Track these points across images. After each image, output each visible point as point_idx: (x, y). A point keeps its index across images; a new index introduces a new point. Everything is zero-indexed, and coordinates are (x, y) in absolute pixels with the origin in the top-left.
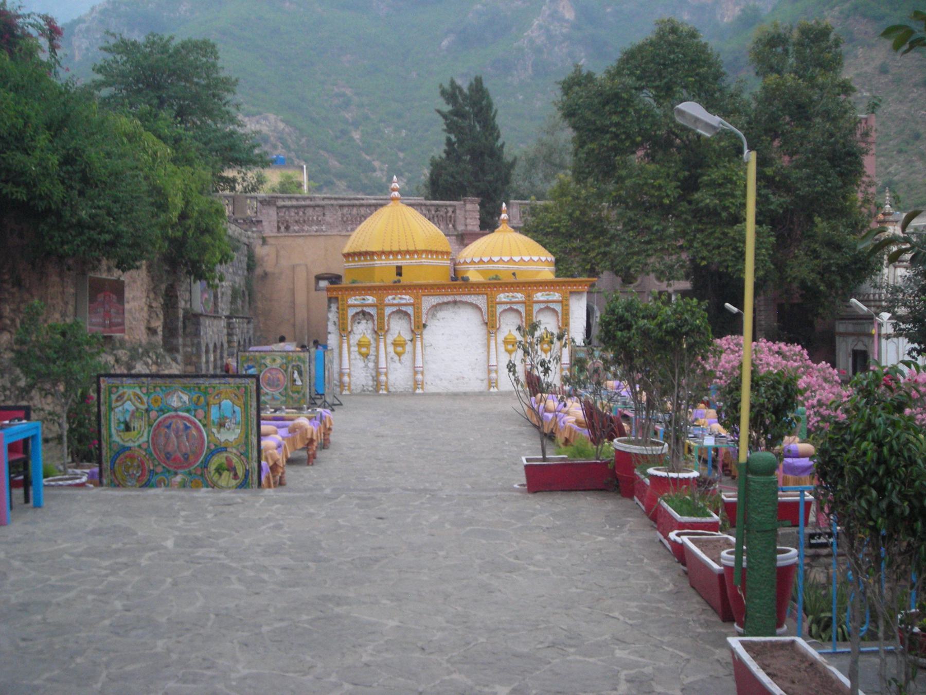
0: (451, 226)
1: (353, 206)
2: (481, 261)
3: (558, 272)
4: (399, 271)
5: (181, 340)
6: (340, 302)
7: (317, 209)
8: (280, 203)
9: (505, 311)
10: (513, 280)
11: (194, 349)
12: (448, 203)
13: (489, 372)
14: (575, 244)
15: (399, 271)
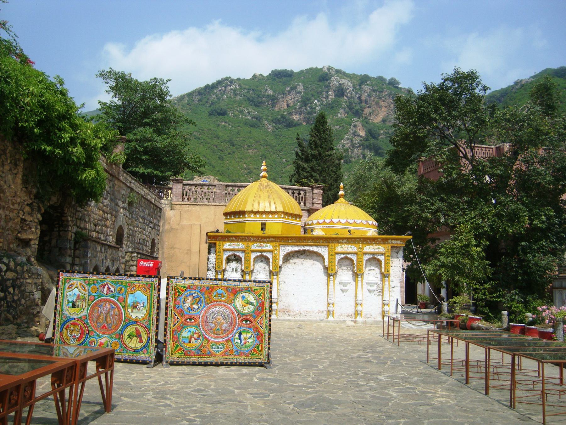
0: (302, 203)
1: (235, 186)
2: (324, 222)
3: (379, 234)
4: (263, 227)
5: (69, 260)
6: (217, 247)
7: (210, 187)
8: (184, 182)
9: (342, 259)
10: (348, 235)
11: (81, 268)
12: (301, 188)
13: (329, 304)
14: (391, 214)
15: (263, 227)
